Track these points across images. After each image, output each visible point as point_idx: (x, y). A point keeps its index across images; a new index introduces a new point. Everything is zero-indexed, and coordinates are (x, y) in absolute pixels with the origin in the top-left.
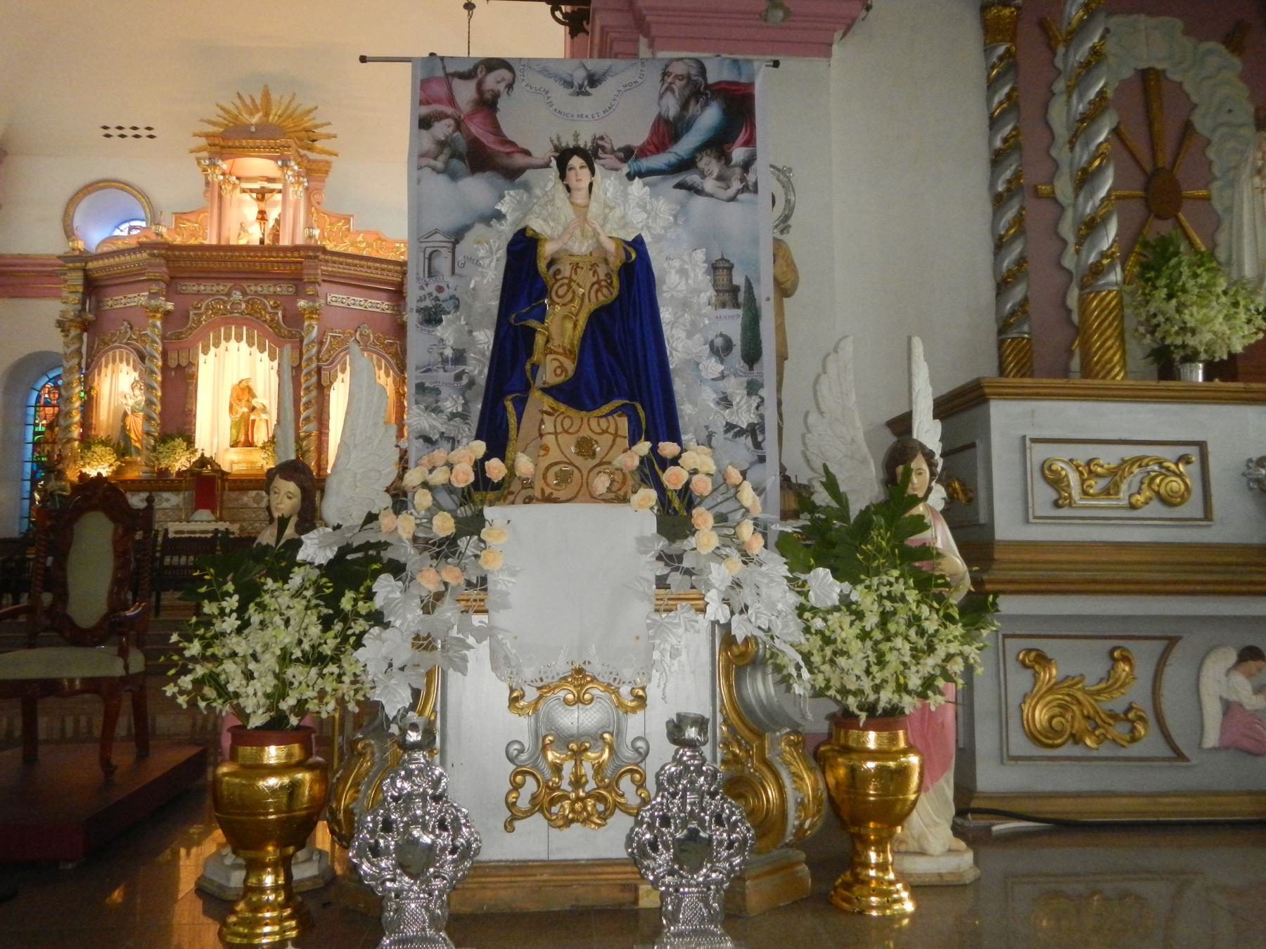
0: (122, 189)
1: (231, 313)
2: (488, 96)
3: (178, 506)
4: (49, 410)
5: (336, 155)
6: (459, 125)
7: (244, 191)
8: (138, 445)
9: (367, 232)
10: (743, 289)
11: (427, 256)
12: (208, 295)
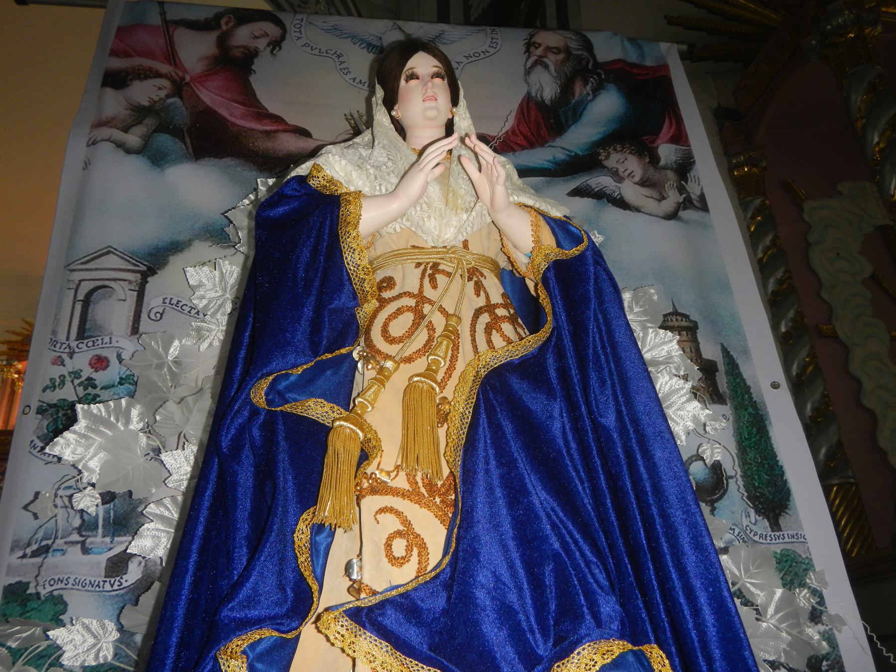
2: (238, 53)
6: (179, 88)
10: (721, 367)
11: (81, 297)
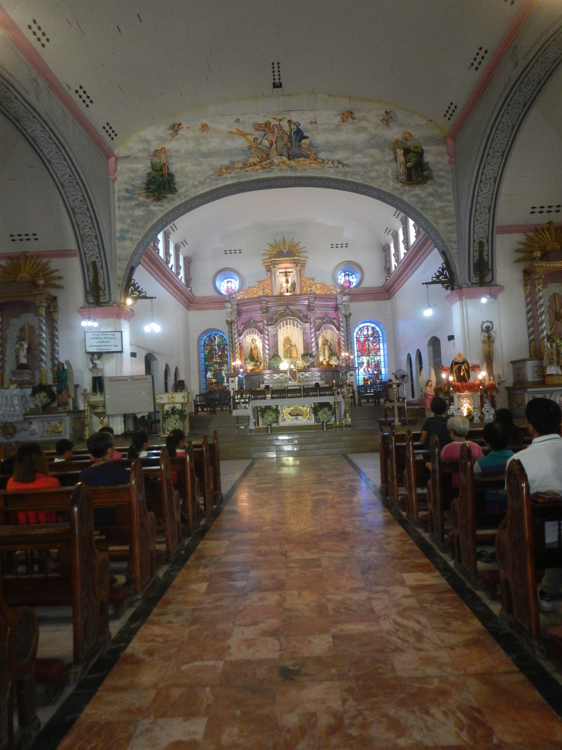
0: (231, 271)
1: (286, 316)
3: (279, 378)
4: (208, 347)
5: (308, 258)
7: (280, 273)
8: (257, 359)
9: (320, 284)
12: (279, 311)
